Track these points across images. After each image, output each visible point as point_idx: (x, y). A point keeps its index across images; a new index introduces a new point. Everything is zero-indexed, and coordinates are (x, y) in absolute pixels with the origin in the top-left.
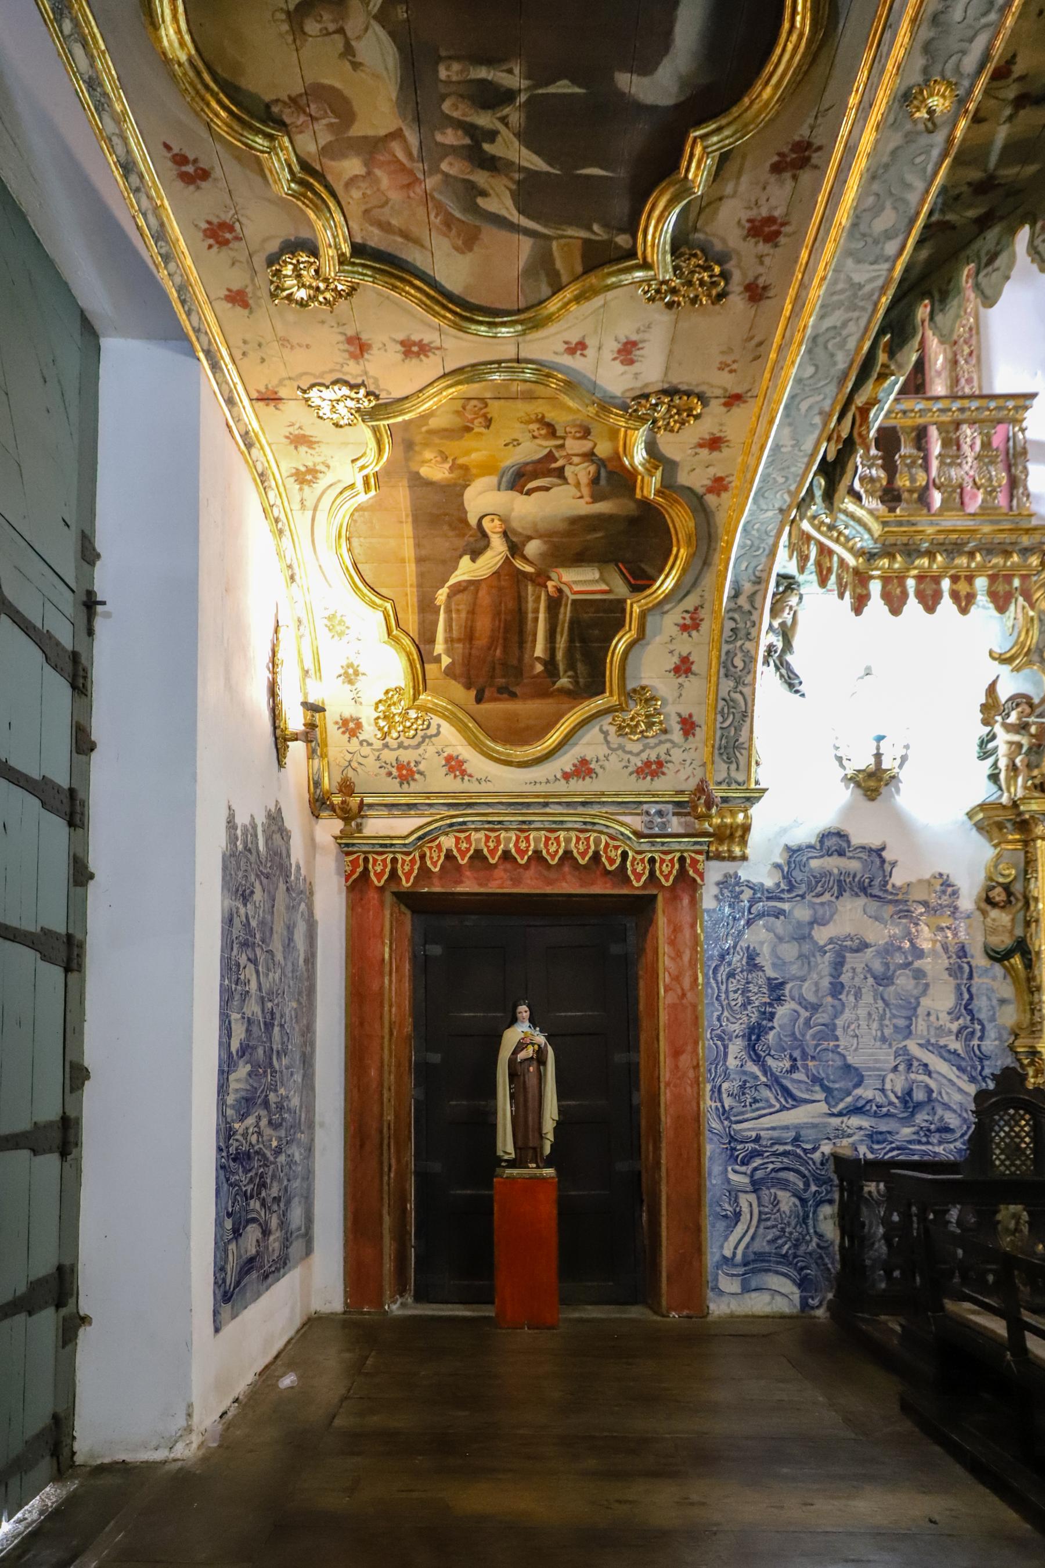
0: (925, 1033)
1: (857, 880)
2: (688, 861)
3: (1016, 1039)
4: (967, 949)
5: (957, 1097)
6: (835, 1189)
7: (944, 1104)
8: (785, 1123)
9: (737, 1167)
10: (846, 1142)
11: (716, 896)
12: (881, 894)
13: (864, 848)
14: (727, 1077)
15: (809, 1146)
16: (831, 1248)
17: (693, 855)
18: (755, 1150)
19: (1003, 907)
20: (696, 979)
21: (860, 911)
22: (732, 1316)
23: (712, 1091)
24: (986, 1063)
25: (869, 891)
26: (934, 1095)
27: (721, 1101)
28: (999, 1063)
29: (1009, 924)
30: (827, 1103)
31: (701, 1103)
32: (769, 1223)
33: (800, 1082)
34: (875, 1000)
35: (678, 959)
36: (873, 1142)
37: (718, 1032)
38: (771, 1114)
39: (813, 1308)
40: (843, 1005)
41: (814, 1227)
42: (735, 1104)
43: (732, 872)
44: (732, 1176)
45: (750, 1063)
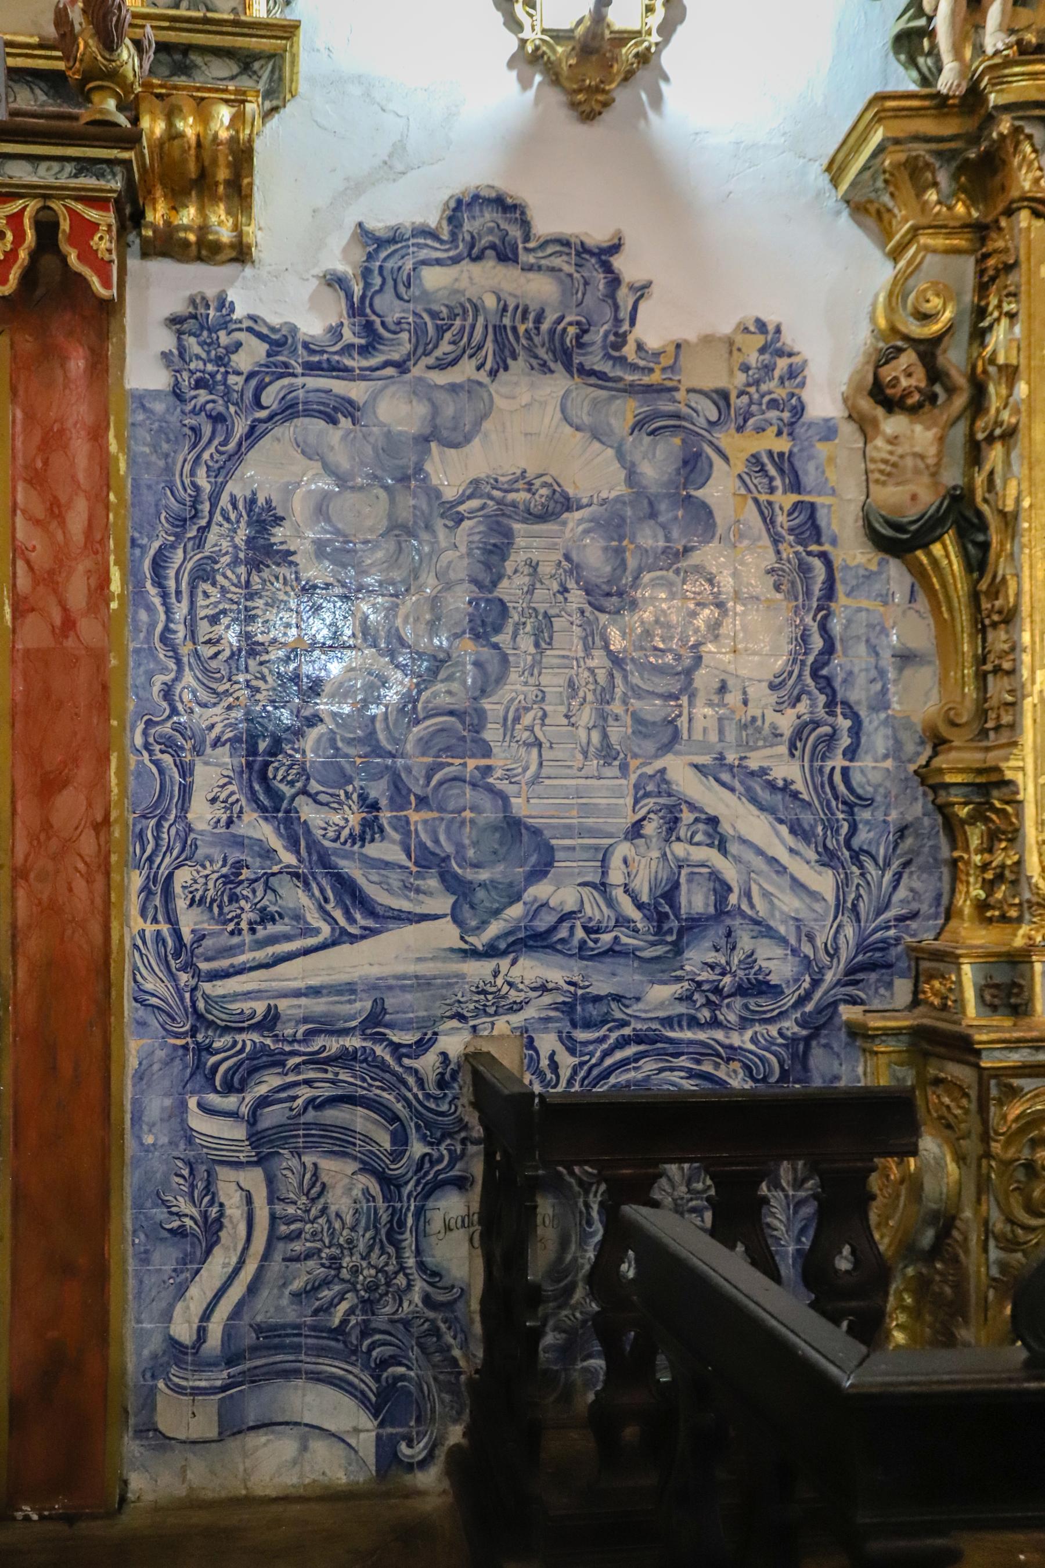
0: (713, 737)
1: (545, 327)
4: (821, 516)
6: (472, 1149)
8: (344, 978)
9: (214, 1099)
10: (503, 1025)
12: (606, 367)
13: (567, 244)
14: (188, 852)
15: (408, 1038)
16: (460, 1305)
18: (260, 1051)
19: (913, 410)
20: (106, 580)
22: (193, 1503)
24: (864, 815)
25: (576, 360)
27: (172, 920)
29: (932, 451)
30: (457, 920)
32: (298, 1247)
33: (387, 865)
34: (587, 649)
37: (166, 729)
38: (307, 952)
40: (504, 659)
41: (418, 1252)
43: (211, 293)
44: (199, 1123)
45: (251, 816)
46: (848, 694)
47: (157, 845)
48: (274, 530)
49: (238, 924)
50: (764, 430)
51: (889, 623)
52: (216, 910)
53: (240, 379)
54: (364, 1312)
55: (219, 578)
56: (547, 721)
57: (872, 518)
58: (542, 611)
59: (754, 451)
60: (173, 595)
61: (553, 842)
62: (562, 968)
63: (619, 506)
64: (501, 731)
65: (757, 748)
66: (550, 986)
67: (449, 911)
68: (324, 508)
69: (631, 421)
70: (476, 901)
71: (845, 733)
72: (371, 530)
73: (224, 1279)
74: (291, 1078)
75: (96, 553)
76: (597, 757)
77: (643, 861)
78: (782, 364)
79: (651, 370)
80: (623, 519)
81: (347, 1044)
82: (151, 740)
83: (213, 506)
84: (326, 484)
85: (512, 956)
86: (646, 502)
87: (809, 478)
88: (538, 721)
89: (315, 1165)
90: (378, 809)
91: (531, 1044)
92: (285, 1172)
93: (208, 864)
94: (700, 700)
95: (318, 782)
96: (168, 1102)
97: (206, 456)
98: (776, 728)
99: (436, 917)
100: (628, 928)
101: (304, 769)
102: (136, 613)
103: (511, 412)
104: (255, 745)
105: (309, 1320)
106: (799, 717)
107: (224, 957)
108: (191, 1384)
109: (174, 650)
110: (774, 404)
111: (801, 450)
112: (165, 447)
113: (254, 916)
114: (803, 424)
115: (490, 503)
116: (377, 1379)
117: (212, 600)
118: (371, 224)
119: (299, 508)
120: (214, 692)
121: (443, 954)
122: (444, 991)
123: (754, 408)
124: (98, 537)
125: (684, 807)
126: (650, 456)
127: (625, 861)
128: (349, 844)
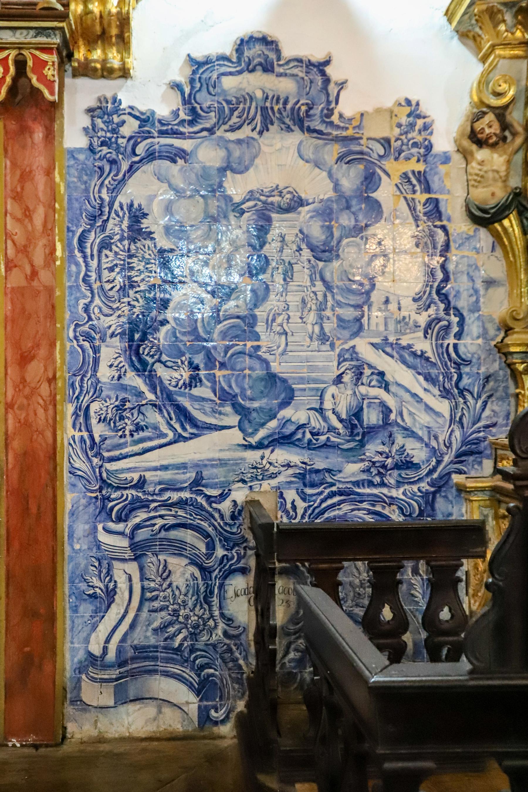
0: (382, 328)
1: (289, 107)
2: (30, 63)
3: (506, 335)
5: (424, 419)
6: (250, 552)
7: (406, 429)
8: (180, 460)
9: (112, 525)
10: (266, 485)
11: (85, 129)
13: (300, 61)
15: (215, 492)
16: (243, 637)
17: (37, 53)
19: (494, 146)
21: (293, 151)
23: (76, 414)
25: (306, 124)
26: (393, 416)
27: (89, 430)
28: (483, 370)
29: (504, 168)
30: (241, 429)
31: (59, 433)
32: (156, 604)
33: (203, 399)
35: (27, 220)
36: (305, 485)
37: (86, 328)
39: (216, 723)
41: (221, 608)
42: (108, 433)
44: (103, 537)
46: (457, 303)
47: (81, 390)
48: (142, 221)
49: (124, 432)
50: (409, 159)
51: (480, 264)
52: (112, 424)
53: (125, 141)
54: (192, 640)
55: (114, 247)
56: (290, 321)
57: (470, 206)
58: (287, 261)
59: (404, 171)
60: (89, 257)
61: (294, 386)
62: (298, 454)
63: (329, 203)
64: (266, 326)
65: (406, 334)
66: (292, 464)
67: (237, 424)
68: (170, 208)
69: (336, 157)
70: (251, 418)
71: (455, 325)
72: (195, 219)
73: (117, 621)
74: (152, 514)
75: (49, 235)
78: (420, 123)
79: (347, 128)
80: (331, 209)
81: (182, 496)
82: (78, 334)
83: (111, 208)
84: (171, 195)
85: (271, 448)
86: (344, 200)
87: (435, 185)
88: (285, 321)
89: (165, 561)
90: (199, 370)
91: (281, 496)
92: (149, 564)
93: (108, 400)
94: (374, 308)
95: (167, 355)
96: (87, 527)
97: (106, 182)
98: (416, 322)
99: (230, 427)
100: (335, 433)
101: (159, 349)
102: (69, 266)
103: (271, 153)
104: (133, 336)
105: (162, 644)
106: (429, 316)
107: (116, 450)
108: (100, 676)
109: (90, 286)
110: (415, 145)
111: (431, 169)
112: (85, 178)
113: (132, 428)
114: (432, 155)
116: (199, 676)
117: (110, 259)
118: (194, 55)
119: (156, 209)
120: (111, 308)
121: (234, 447)
122: (234, 467)
123: (404, 147)
124: (49, 227)
126: (346, 175)
127: (333, 396)
128: (183, 388)
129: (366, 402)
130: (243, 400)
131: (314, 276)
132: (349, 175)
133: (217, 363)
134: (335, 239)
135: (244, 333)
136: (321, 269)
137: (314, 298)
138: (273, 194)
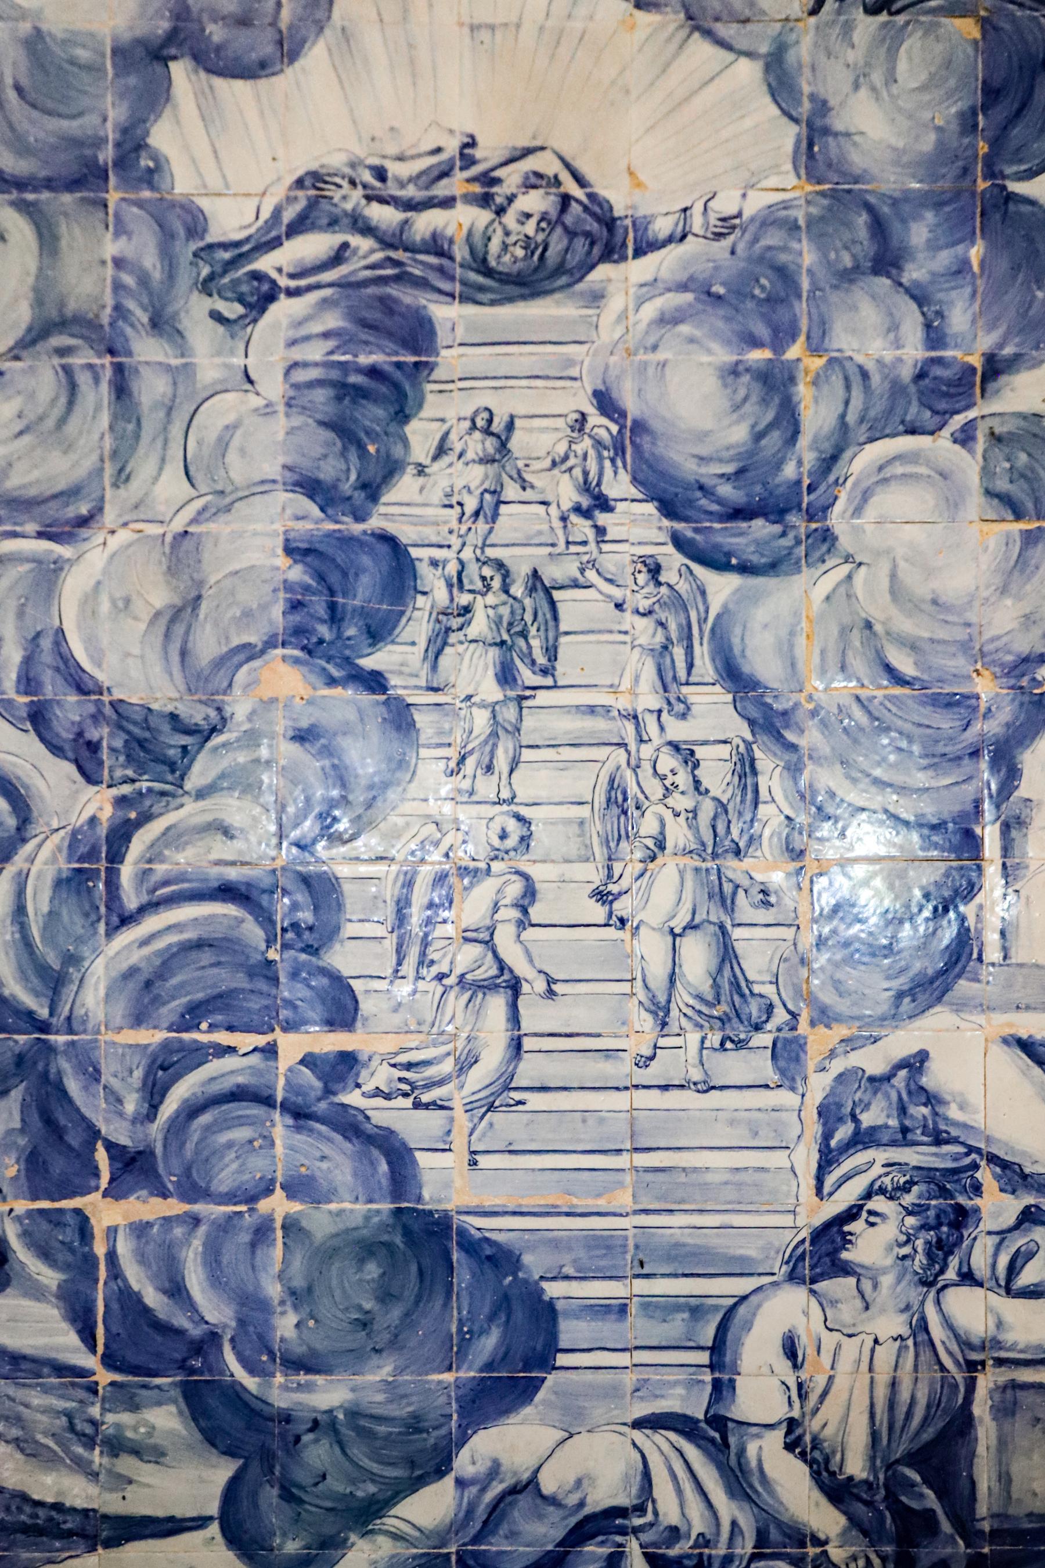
56: (536, 913)
58: (521, 571)
61: (553, 1290)
63: (773, 238)
64: (390, 944)
67: (213, 1509)
70: (301, 1476)
76: (701, 1019)
77: (850, 1348)
80: (785, 275)
86: (862, 219)
115: (362, 244)
125: (985, 1175)
126: (877, 77)
127: (791, 1349)
129: (985, 1383)
130: (252, 1369)
131: (679, 653)
132: (891, 78)
133: (101, 1156)
134: (804, 441)
135: (262, 985)
136: (719, 616)
137: (683, 779)
138: (441, 190)
